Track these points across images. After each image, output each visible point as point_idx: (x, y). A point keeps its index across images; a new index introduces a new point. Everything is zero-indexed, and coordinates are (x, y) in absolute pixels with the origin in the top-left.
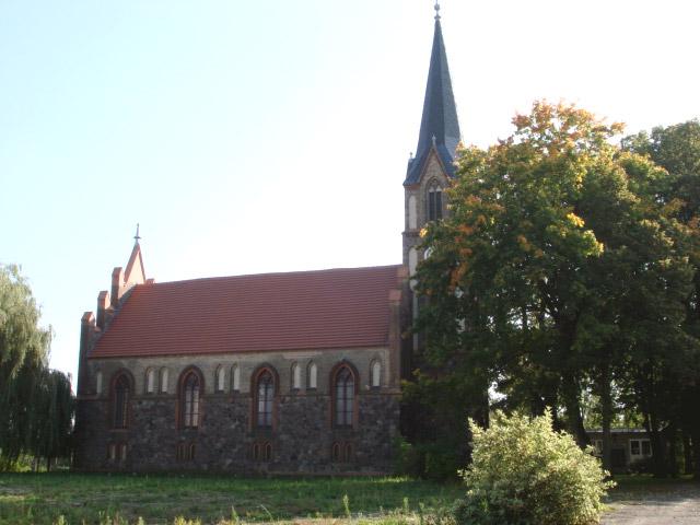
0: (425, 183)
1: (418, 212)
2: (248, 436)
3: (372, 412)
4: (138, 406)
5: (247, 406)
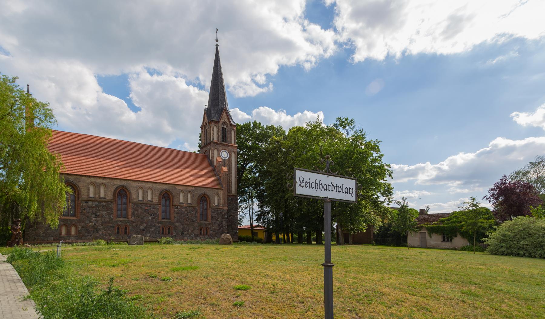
0: (221, 122)
1: (218, 134)
2: (158, 223)
3: (216, 216)
4: (85, 204)
5: (158, 209)
